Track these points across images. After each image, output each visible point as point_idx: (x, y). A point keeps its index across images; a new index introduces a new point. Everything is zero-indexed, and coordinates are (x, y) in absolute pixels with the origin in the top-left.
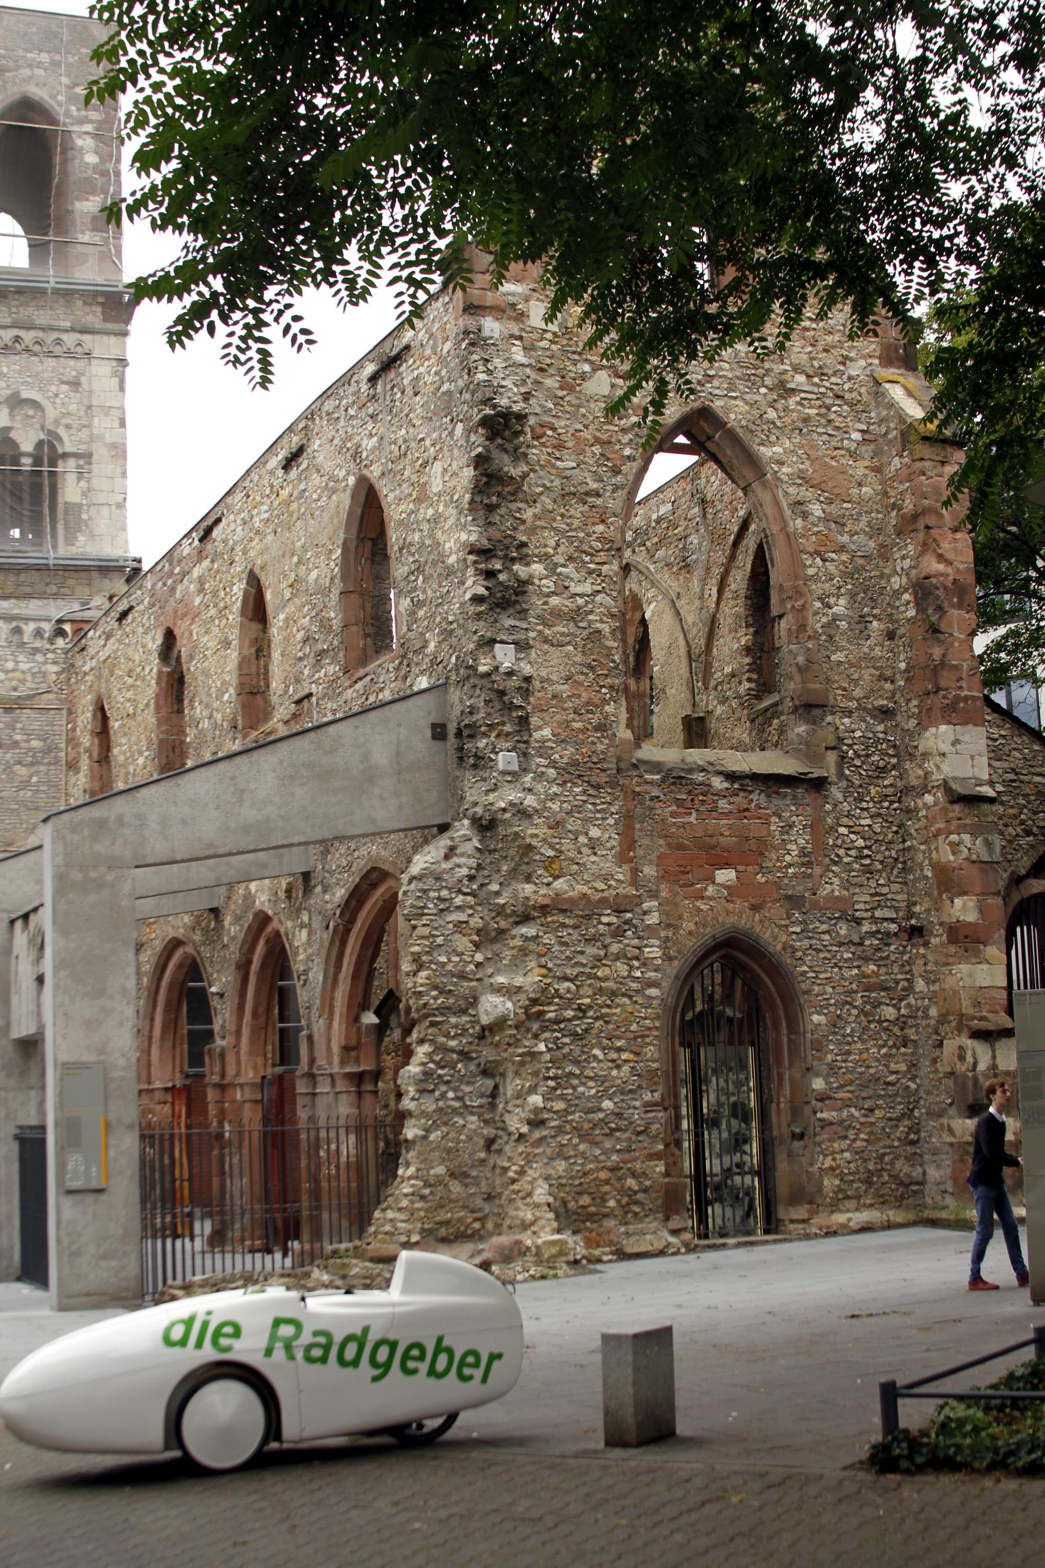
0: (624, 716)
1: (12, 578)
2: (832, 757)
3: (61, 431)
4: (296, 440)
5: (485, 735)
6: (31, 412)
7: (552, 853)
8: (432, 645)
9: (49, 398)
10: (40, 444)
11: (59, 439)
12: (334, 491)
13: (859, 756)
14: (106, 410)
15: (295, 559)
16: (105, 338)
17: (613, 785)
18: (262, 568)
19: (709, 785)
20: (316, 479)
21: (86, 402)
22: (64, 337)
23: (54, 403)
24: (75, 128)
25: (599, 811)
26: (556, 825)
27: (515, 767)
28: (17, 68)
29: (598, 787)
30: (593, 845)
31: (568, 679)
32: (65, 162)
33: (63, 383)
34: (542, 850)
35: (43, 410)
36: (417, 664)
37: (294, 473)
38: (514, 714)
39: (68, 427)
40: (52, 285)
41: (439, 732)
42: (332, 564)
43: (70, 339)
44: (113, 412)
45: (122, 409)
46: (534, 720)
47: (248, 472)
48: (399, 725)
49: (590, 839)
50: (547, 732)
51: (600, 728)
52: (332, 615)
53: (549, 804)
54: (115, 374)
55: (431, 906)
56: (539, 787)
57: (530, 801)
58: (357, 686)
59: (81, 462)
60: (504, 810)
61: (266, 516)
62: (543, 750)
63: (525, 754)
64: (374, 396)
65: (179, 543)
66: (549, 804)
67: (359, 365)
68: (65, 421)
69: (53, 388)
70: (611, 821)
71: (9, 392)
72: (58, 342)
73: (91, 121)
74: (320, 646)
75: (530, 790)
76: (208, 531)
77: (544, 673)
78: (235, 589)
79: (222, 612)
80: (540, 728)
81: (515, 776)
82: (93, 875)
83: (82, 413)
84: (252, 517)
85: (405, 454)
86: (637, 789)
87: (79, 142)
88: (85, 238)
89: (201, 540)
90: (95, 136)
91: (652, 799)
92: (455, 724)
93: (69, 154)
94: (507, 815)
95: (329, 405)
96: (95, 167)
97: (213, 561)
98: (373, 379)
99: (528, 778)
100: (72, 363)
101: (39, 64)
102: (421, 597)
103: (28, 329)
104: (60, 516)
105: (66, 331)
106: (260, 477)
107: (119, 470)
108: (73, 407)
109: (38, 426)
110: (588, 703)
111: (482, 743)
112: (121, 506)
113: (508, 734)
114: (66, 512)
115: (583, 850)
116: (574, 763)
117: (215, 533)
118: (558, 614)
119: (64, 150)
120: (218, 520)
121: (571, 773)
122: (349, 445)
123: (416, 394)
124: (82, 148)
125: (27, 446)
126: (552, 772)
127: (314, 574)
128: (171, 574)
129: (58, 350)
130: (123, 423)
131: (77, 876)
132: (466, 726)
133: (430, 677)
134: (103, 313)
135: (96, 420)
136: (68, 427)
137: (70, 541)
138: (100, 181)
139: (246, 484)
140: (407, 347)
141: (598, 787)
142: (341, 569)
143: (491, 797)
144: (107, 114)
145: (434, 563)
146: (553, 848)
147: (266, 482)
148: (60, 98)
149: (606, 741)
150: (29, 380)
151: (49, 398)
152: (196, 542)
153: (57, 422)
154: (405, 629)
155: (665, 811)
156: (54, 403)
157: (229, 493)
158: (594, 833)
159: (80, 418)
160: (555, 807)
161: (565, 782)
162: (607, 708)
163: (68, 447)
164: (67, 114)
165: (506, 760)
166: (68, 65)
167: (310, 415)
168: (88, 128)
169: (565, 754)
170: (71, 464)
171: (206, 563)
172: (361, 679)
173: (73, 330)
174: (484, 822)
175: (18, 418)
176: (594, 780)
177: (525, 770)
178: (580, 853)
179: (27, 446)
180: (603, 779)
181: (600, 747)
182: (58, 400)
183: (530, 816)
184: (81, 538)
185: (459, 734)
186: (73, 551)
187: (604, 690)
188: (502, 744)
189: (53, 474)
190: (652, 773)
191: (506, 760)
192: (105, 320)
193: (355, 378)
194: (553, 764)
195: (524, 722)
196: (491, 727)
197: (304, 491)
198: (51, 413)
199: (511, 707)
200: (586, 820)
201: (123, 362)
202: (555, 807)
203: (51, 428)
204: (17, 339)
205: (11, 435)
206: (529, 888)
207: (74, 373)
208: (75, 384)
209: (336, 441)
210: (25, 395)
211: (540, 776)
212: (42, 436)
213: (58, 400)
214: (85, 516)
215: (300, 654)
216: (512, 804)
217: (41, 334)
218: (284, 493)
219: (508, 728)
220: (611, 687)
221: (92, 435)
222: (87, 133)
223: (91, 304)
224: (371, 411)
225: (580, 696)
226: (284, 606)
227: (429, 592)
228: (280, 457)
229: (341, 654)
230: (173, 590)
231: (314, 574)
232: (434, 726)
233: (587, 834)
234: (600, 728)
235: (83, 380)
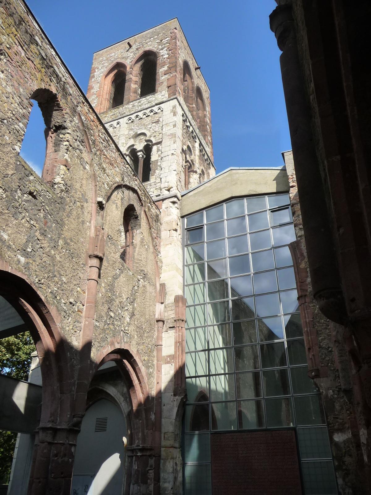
3: (152, 139)
21: (161, 125)
22: (153, 108)
33: (153, 123)
43: (155, 109)
59: (159, 145)
68: (153, 135)
69: (150, 126)
71: (134, 134)
107: (173, 142)
108: (157, 129)
129: (152, 113)
135: (164, 130)
150: (141, 127)
153: (151, 136)
163: (154, 142)
173: (157, 105)
198: (148, 134)
204: (137, 116)
205: (134, 148)
207: (157, 119)
208: (158, 122)
210: (139, 133)
213: (151, 129)
214: (159, 164)
217: (145, 111)
235: (161, 120)
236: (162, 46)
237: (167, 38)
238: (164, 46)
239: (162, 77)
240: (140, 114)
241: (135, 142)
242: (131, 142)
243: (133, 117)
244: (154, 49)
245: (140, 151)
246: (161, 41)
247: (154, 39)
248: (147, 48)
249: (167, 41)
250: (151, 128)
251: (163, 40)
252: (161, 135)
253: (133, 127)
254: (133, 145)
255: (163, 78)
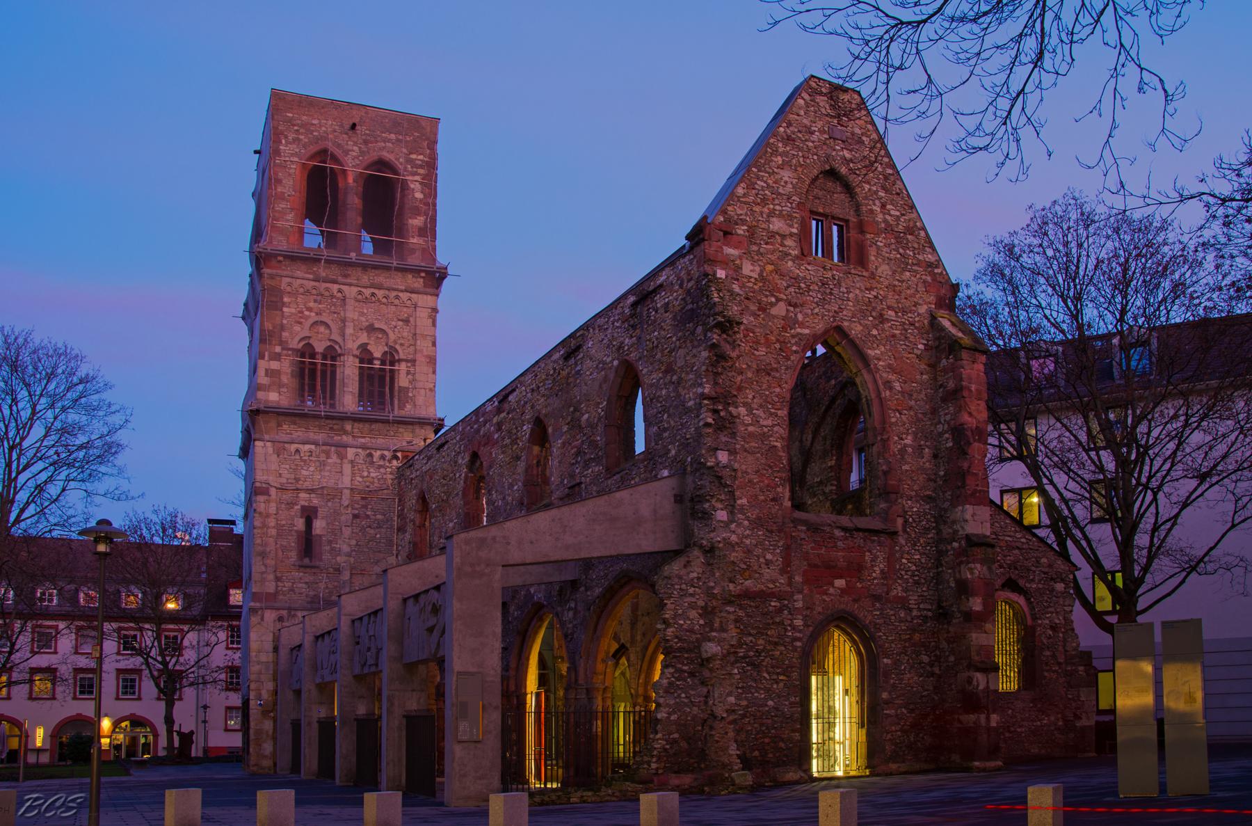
0: (787, 494)
1: (367, 425)
2: (900, 521)
4: (573, 343)
5: (708, 501)
6: (380, 336)
7: (745, 567)
8: (673, 452)
9: (391, 328)
10: (385, 353)
11: (397, 351)
12: (603, 369)
13: (915, 522)
14: (424, 336)
15: (572, 409)
16: (425, 297)
17: (780, 531)
18: (546, 415)
19: (833, 534)
20: (588, 363)
22: (401, 294)
23: (394, 331)
24: (410, 178)
25: (771, 545)
26: (749, 551)
27: (725, 518)
28: (376, 142)
29: (771, 532)
30: (768, 563)
31: (757, 472)
32: (403, 196)
33: (399, 320)
34: (740, 565)
35: (387, 335)
36: (661, 463)
37: (572, 361)
38: (726, 490)
39: (402, 345)
40: (395, 265)
41: (679, 499)
42: (600, 410)
43: (404, 296)
44: (428, 338)
45: (434, 337)
46: (737, 493)
47: (537, 362)
48: (656, 495)
49: (766, 560)
50: (744, 501)
51: (773, 500)
52: (599, 438)
53: (744, 540)
54: (430, 317)
55: (675, 592)
56: (739, 531)
57: (734, 538)
58: (615, 478)
60: (719, 542)
61: (550, 386)
62: (742, 510)
63: (732, 513)
64: (634, 315)
65: (484, 404)
66: (744, 540)
67: (624, 297)
68: (399, 342)
69: (394, 323)
70: (778, 551)
71: (367, 324)
72: (397, 297)
73: (419, 174)
74: (588, 456)
75: (734, 532)
76: (506, 397)
77: (744, 467)
78: (525, 428)
79: (514, 442)
80: (741, 498)
81: (727, 524)
82: (478, 569)
83: (410, 338)
84: (538, 387)
85: (657, 346)
86: (793, 534)
87: (412, 186)
88: (415, 241)
89: (499, 402)
90: (421, 183)
91: (801, 539)
92: (690, 495)
93: (406, 192)
94: (721, 545)
95: (601, 321)
96: (421, 200)
97: (508, 413)
98: (634, 305)
99: (733, 526)
100: (405, 309)
101: (390, 140)
102: (666, 426)
103: (380, 289)
104: (396, 394)
105: (402, 291)
106: (546, 364)
109: (384, 344)
110: (768, 486)
111: (706, 505)
112: (432, 390)
113: (722, 500)
114: (399, 392)
115: (762, 566)
116: (759, 518)
117: (510, 398)
118: (751, 435)
119: (403, 190)
120: (514, 390)
121: (757, 523)
122: (615, 343)
123: (666, 312)
124: (413, 189)
125: (377, 354)
126: (746, 523)
127: (586, 416)
128: (477, 421)
129: (397, 302)
130: (434, 344)
131: (468, 569)
132: (697, 496)
133: (671, 469)
134: (424, 282)
136: (402, 345)
137: (401, 407)
138: (423, 208)
139: (536, 369)
140: (661, 286)
141: (771, 532)
142: (606, 413)
143: (712, 535)
144: (429, 171)
145: (677, 407)
146: (745, 563)
147: (550, 368)
148: (401, 160)
149: (777, 507)
151: (391, 328)
152: (496, 403)
153: (395, 342)
154: (653, 444)
155: (808, 547)
156: (394, 331)
157: (521, 375)
158: (769, 557)
159: (409, 340)
160: (748, 542)
161: (753, 528)
162: (778, 489)
163: (402, 356)
164: (405, 169)
165: (722, 515)
166: (407, 142)
167: (586, 327)
168: (417, 178)
169: (753, 514)
170: (403, 367)
171: (503, 415)
172: (618, 473)
174: (707, 549)
175: (373, 339)
176: (769, 528)
177: (732, 522)
178: (760, 567)
179: (377, 354)
180: (775, 528)
181: (773, 511)
182: (396, 330)
183: (733, 547)
184: (408, 406)
185: (692, 500)
186: (403, 413)
187: (777, 479)
188: (719, 505)
189: (392, 371)
190: (802, 526)
191: (722, 515)
192: (425, 286)
193: (621, 305)
194: (747, 519)
195: (732, 493)
196: (712, 496)
197: (580, 371)
199: (726, 486)
200: (764, 549)
201: (435, 310)
202: (748, 542)
203: (392, 344)
204: (373, 294)
206: (731, 586)
207: (406, 315)
208: (407, 321)
209: (605, 342)
211: (739, 525)
212: (386, 349)
213: (396, 330)
215: (574, 461)
216: (724, 539)
217: (387, 292)
218: (564, 373)
219: (723, 497)
220: (781, 478)
221: (416, 350)
222: (416, 181)
223: (417, 278)
224: (632, 323)
225: (763, 481)
226: (562, 436)
227: (672, 422)
228: (562, 352)
229: (604, 460)
230: (478, 431)
231: (586, 416)
232: (675, 496)
233: (764, 557)
234: (773, 500)
235: (411, 319)
236: (412, 167)
237: (421, 154)
238: (415, 170)
239: (413, 237)
240: (380, 293)
241: (369, 337)
242: (363, 338)
243: (367, 292)
244: (397, 162)
245: (378, 359)
246: (411, 153)
247: (398, 140)
248: (386, 155)
249: (420, 162)
250: (395, 327)
251: (412, 153)
252: (412, 348)
253: (365, 311)
254: (367, 344)
255: (415, 241)
